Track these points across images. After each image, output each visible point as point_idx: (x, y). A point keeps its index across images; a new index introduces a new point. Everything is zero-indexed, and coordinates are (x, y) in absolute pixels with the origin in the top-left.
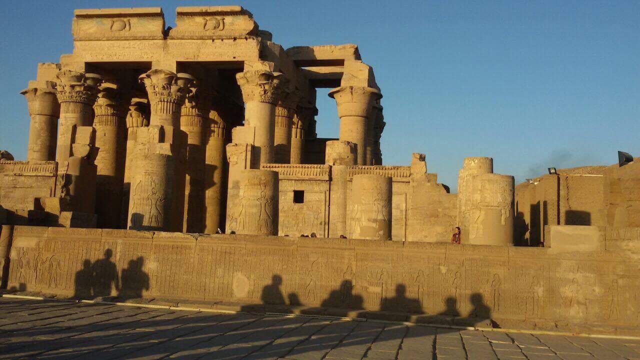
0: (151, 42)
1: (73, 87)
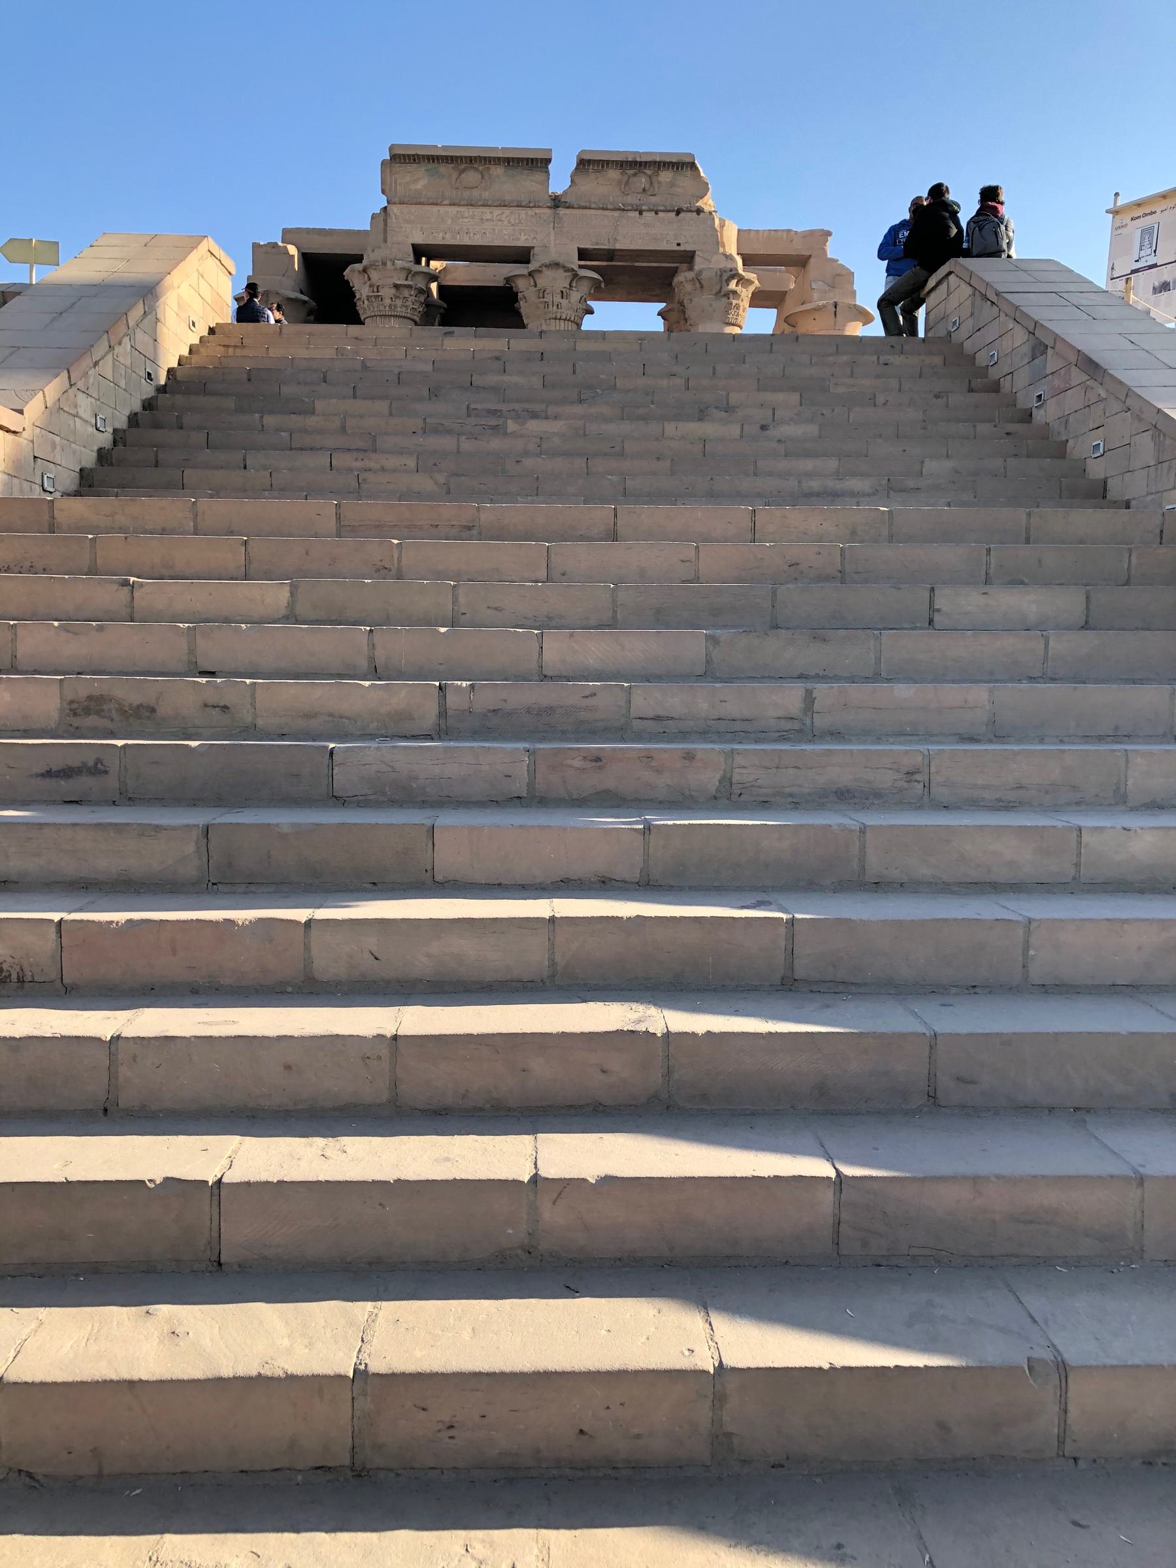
0: (530, 212)
1: (396, 286)
